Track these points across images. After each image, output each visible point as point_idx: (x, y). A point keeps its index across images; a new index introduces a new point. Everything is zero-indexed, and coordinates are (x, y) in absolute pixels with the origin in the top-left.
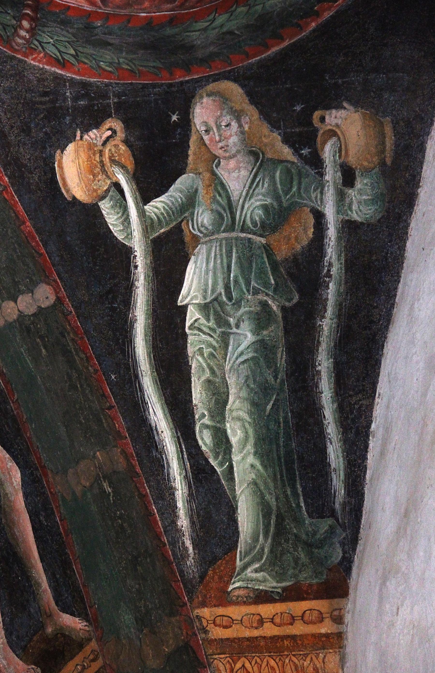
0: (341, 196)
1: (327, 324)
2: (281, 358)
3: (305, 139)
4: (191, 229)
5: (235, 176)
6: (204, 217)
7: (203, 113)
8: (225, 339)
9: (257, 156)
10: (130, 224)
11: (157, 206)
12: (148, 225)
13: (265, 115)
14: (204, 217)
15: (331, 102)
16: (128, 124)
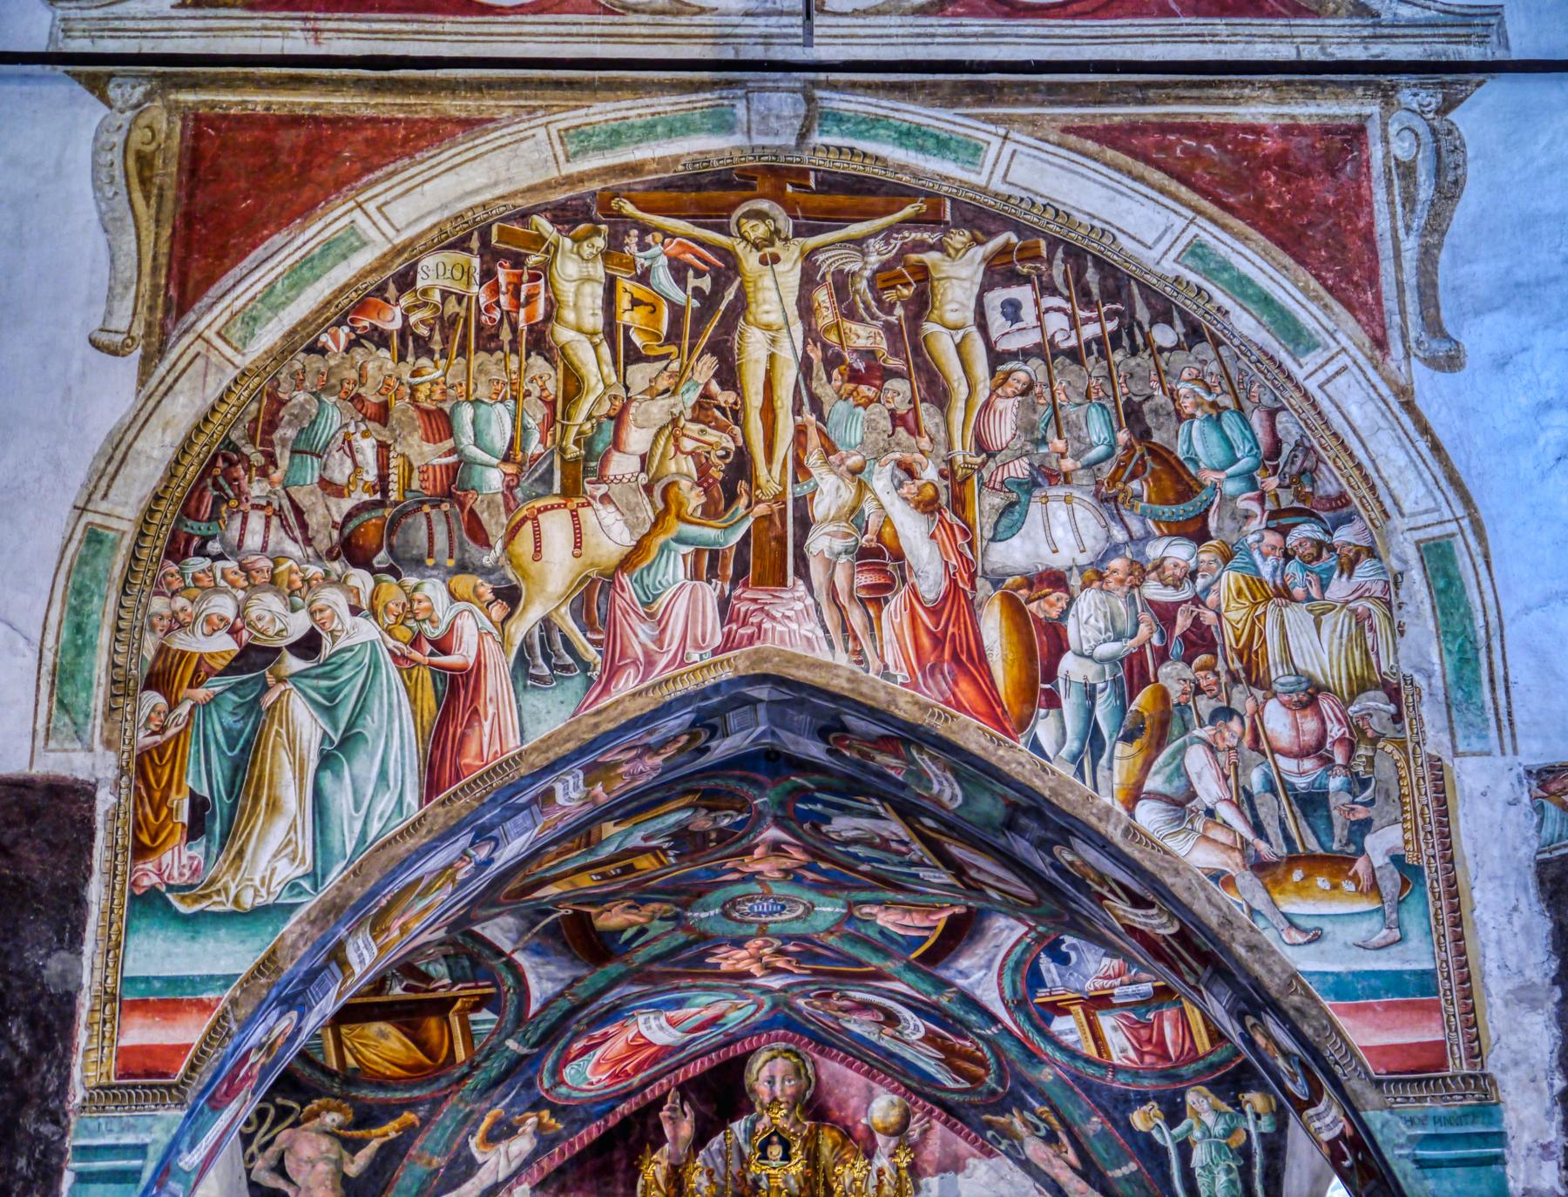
0: (1256, 1124)
1: (1257, 1171)
2: (1239, 1185)
3: (1237, 1104)
4: (1191, 1139)
5: (1209, 1119)
6: (1197, 1134)
7: (1191, 1097)
8: (1213, 1179)
9: (1219, 1113)
10: (1166, 1138)
11: (1176, 1131)
12: (1173, 1138)
13: (1218, 1096)
14: (1197, 1134)
15: (1246, 1090)
16: (1159, 1103)
